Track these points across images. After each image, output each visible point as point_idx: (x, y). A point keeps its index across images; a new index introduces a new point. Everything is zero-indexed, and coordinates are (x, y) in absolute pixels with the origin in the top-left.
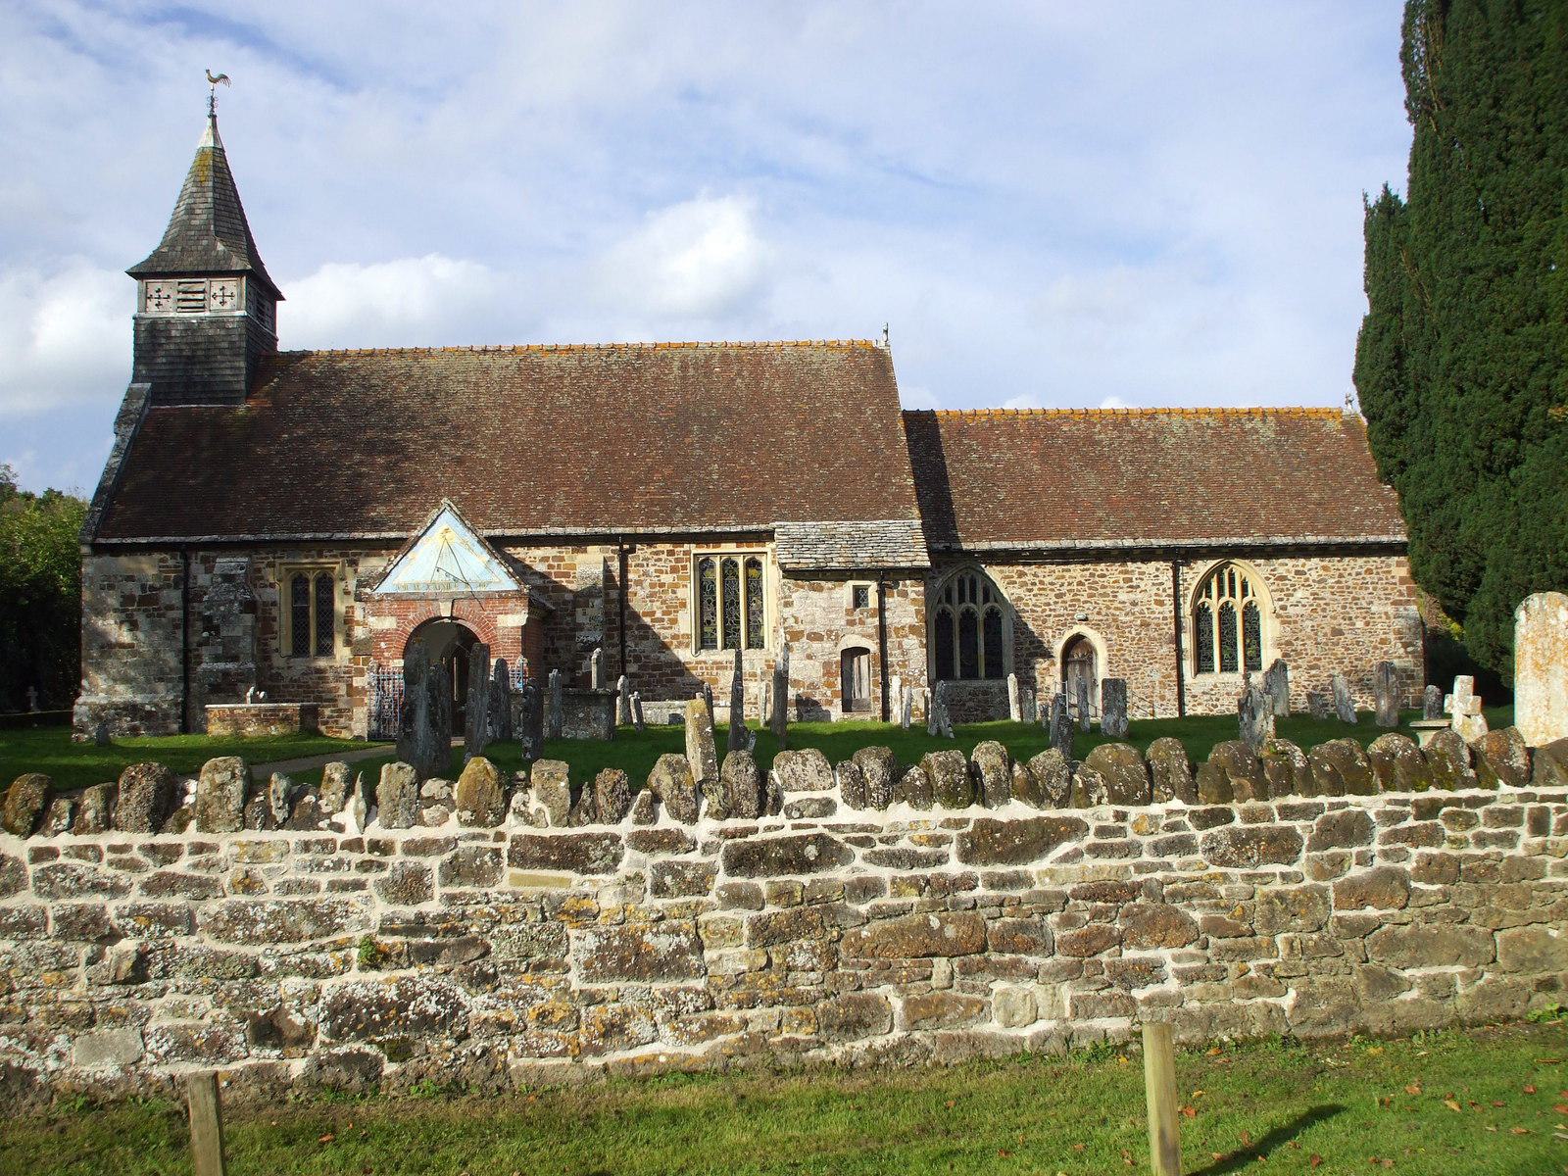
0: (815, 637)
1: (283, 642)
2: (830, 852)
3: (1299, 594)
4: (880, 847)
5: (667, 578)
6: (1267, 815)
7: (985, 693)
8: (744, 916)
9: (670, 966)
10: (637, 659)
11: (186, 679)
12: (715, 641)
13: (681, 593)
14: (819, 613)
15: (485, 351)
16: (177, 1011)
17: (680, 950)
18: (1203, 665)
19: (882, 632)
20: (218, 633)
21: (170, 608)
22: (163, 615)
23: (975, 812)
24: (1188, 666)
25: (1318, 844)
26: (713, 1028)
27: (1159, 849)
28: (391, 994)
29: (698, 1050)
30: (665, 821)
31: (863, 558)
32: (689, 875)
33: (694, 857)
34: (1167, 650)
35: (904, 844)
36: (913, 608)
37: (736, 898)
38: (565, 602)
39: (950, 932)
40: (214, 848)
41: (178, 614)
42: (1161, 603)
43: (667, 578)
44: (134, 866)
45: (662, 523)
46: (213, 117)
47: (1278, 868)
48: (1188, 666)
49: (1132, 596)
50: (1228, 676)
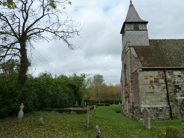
11: (169, 101)
20: (181, 89)
21: (162, 84)
22: (160, 85)
41: (164, 85)
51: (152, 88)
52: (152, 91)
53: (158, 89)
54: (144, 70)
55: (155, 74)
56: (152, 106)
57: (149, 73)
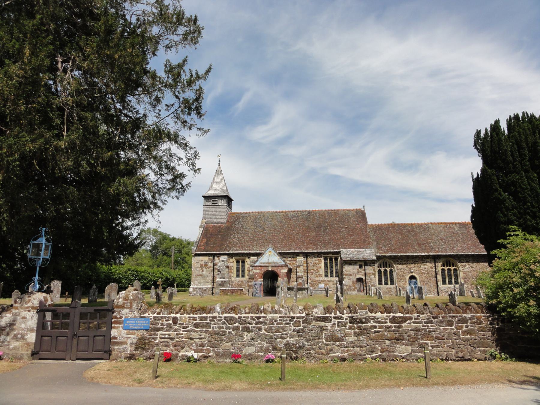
0: (351, 275)
1: (234, 274)
2: (367, 321)
3: (467, 266)
4: (375, 320)
5: (317, 262)
6: (446, 317)
7: (390, 288)
8: (352, 331)
9: (340, 339)
10: (310, 279)
11: (213, 283)
12: (328, 275)
13: (320, 265)
14: (351, 270)
15: (276, 212)
16: (260, 344)
17: (343, 337)
18: (444, 282)
19: (365, 273)
21: (210, 267)
23: (392, 314)
24: (440, 283)
25: (457, 323)
26: (347, 351)
27: (425, 323)
28: (295, 343)
29: (346, 354)
30: (339, 314)
31: (361, 258)
32: (343, 323)
33: (344, 320)
34: (434, 279)
35: (380, 320)
36: (372, 269)
37: (351, 328)
38: (295, 267)
39: (389, 335)
40: (267, 317)
42: (432, 268)
43: (317, 262)
44: (254, 320)
45: (316, 249)
46: (219, 164)
47: (450, 327)
48: (440, 283)
49: (425, 266)
50: (450, 286)
51: (201, 271)
52: (201, 274)
53: (207, 271)
54: (196, 255)
55: (206, 259)
56: (199, 287)
57: (201, 258)
